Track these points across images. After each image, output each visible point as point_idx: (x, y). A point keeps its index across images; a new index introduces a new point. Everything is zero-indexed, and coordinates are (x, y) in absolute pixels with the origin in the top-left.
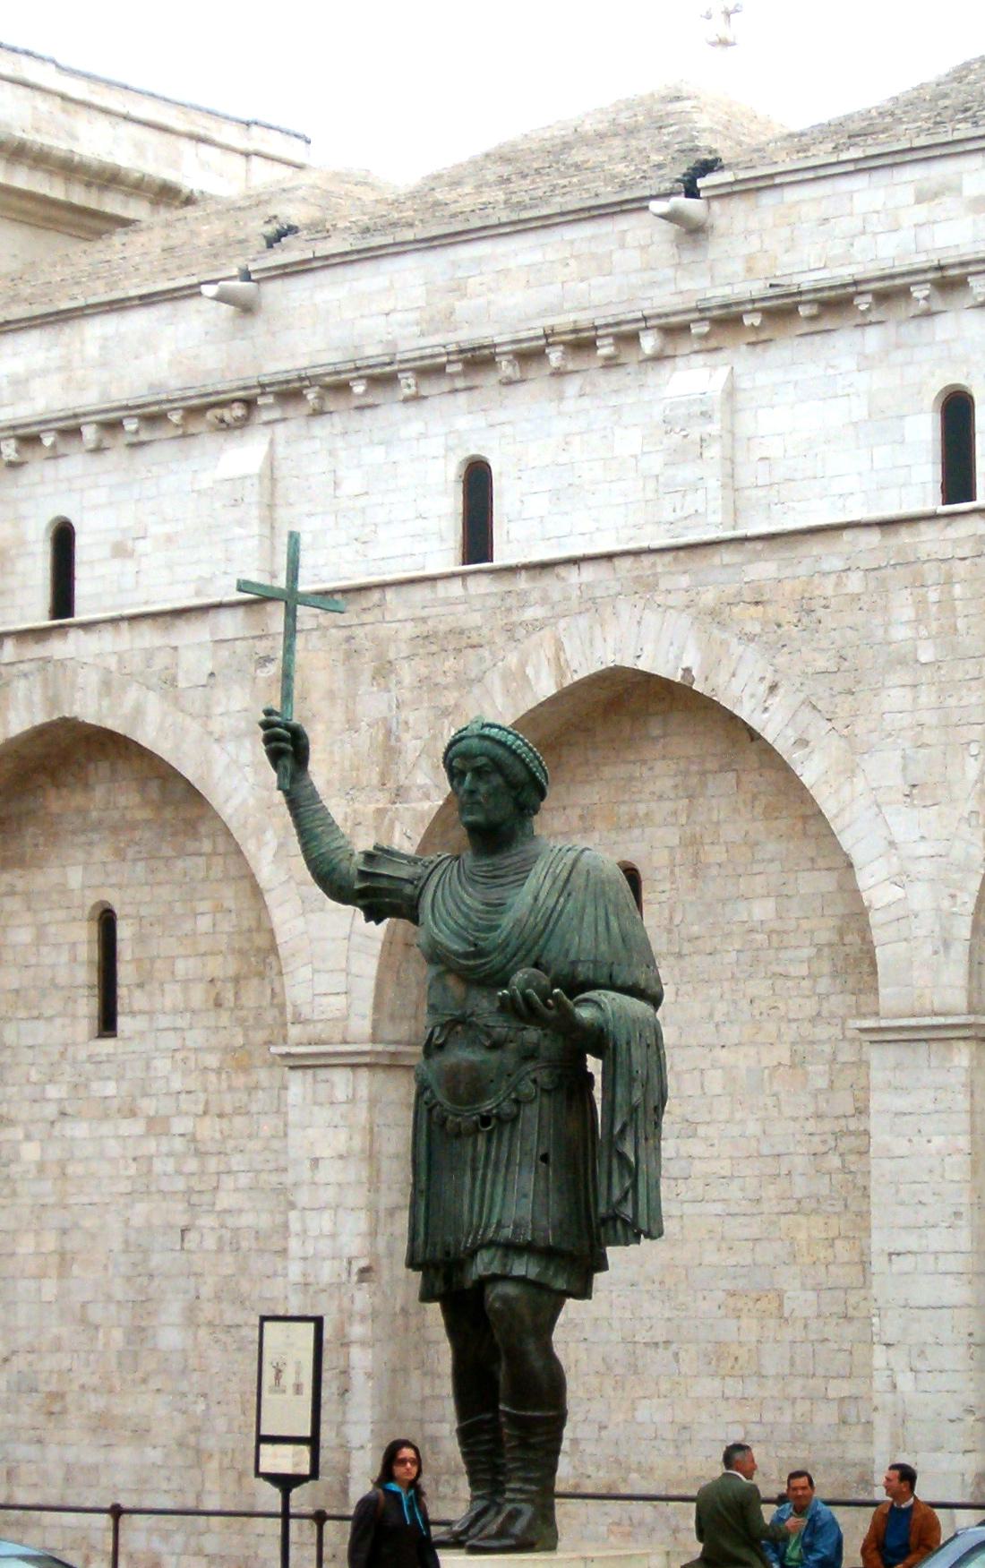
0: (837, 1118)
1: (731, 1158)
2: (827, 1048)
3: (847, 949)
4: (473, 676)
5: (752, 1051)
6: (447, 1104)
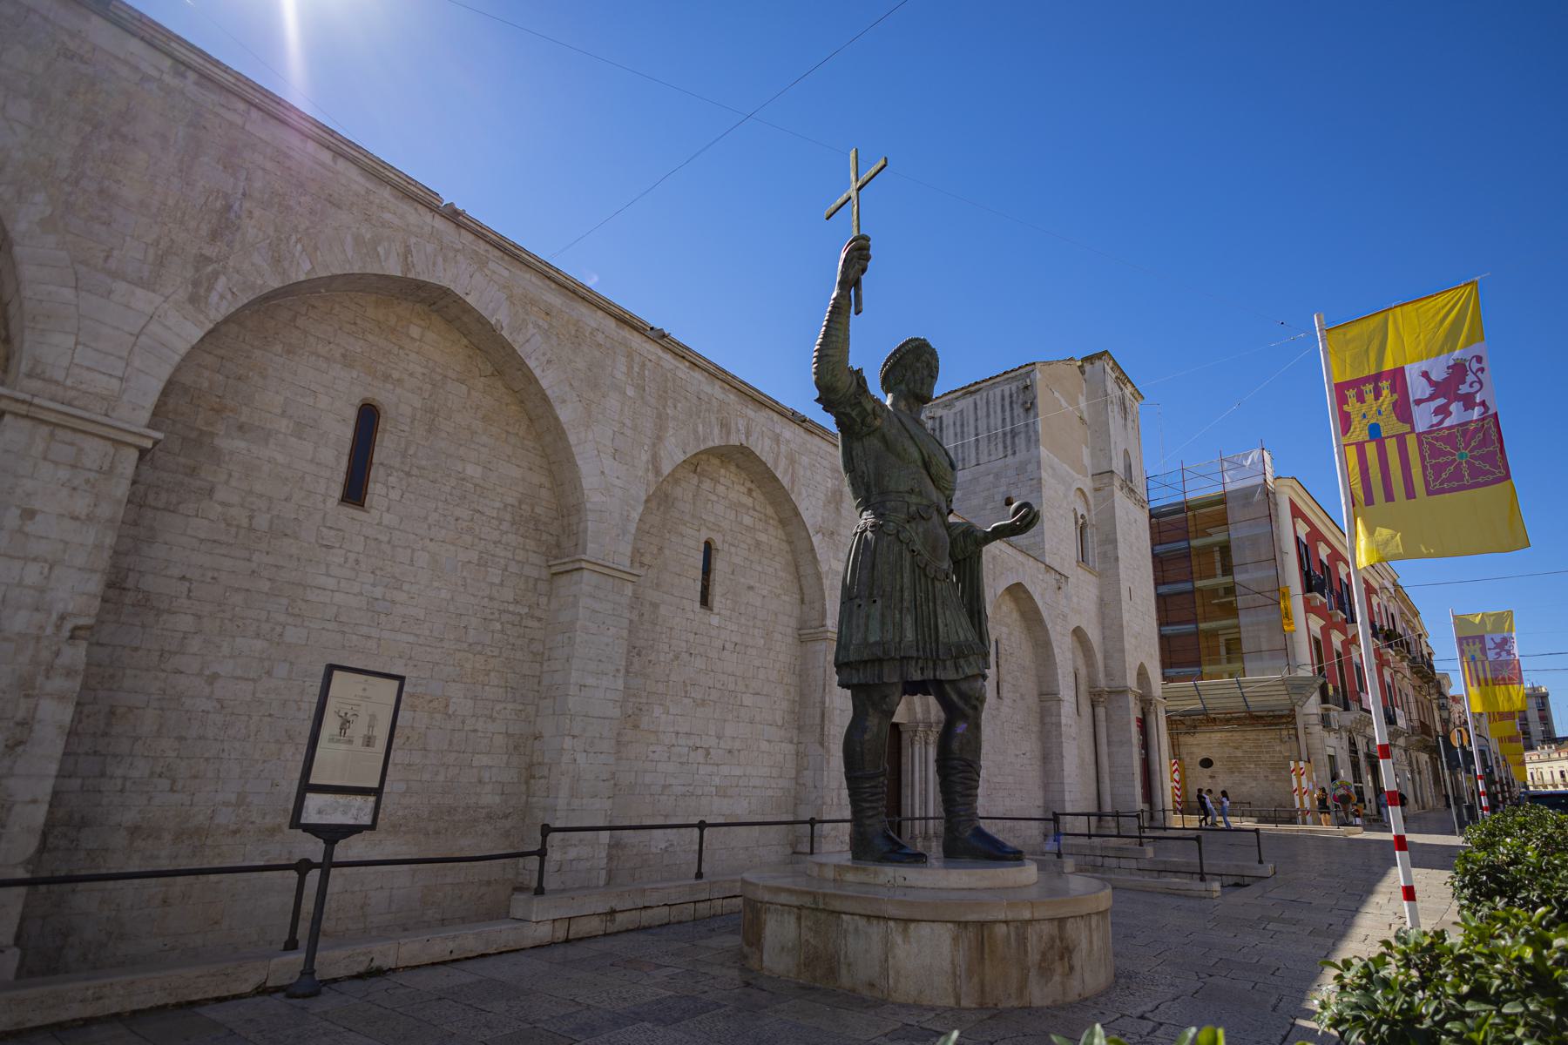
0: (503, 602)
1: (426, 608)
2: (502, 561)
3: (522, 512)
5: (452, 548)
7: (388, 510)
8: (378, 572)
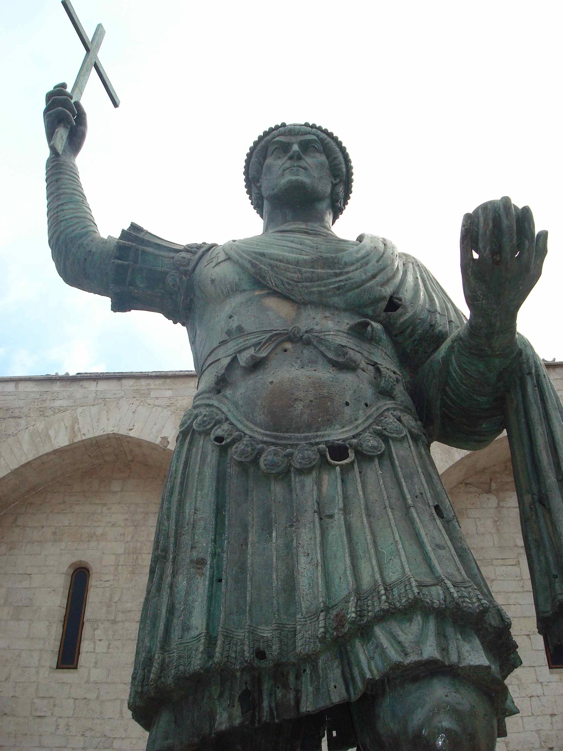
4: (10, 433)
6: (259, 434)
7: (95, 667)
8: (88, 734)
